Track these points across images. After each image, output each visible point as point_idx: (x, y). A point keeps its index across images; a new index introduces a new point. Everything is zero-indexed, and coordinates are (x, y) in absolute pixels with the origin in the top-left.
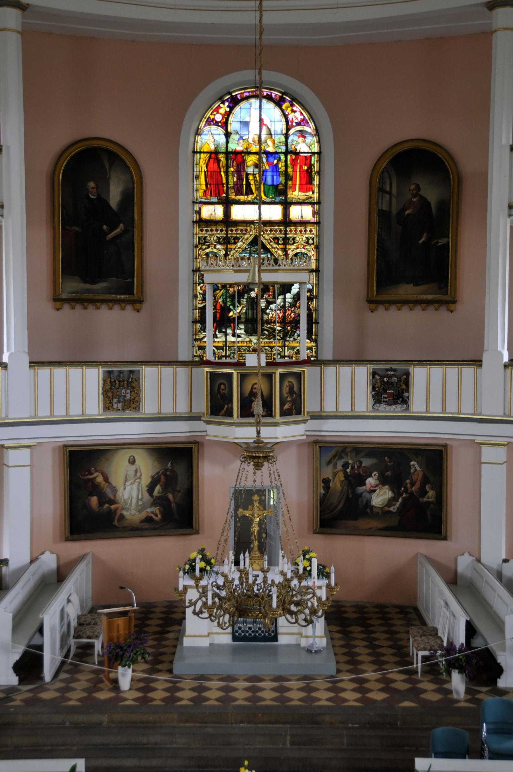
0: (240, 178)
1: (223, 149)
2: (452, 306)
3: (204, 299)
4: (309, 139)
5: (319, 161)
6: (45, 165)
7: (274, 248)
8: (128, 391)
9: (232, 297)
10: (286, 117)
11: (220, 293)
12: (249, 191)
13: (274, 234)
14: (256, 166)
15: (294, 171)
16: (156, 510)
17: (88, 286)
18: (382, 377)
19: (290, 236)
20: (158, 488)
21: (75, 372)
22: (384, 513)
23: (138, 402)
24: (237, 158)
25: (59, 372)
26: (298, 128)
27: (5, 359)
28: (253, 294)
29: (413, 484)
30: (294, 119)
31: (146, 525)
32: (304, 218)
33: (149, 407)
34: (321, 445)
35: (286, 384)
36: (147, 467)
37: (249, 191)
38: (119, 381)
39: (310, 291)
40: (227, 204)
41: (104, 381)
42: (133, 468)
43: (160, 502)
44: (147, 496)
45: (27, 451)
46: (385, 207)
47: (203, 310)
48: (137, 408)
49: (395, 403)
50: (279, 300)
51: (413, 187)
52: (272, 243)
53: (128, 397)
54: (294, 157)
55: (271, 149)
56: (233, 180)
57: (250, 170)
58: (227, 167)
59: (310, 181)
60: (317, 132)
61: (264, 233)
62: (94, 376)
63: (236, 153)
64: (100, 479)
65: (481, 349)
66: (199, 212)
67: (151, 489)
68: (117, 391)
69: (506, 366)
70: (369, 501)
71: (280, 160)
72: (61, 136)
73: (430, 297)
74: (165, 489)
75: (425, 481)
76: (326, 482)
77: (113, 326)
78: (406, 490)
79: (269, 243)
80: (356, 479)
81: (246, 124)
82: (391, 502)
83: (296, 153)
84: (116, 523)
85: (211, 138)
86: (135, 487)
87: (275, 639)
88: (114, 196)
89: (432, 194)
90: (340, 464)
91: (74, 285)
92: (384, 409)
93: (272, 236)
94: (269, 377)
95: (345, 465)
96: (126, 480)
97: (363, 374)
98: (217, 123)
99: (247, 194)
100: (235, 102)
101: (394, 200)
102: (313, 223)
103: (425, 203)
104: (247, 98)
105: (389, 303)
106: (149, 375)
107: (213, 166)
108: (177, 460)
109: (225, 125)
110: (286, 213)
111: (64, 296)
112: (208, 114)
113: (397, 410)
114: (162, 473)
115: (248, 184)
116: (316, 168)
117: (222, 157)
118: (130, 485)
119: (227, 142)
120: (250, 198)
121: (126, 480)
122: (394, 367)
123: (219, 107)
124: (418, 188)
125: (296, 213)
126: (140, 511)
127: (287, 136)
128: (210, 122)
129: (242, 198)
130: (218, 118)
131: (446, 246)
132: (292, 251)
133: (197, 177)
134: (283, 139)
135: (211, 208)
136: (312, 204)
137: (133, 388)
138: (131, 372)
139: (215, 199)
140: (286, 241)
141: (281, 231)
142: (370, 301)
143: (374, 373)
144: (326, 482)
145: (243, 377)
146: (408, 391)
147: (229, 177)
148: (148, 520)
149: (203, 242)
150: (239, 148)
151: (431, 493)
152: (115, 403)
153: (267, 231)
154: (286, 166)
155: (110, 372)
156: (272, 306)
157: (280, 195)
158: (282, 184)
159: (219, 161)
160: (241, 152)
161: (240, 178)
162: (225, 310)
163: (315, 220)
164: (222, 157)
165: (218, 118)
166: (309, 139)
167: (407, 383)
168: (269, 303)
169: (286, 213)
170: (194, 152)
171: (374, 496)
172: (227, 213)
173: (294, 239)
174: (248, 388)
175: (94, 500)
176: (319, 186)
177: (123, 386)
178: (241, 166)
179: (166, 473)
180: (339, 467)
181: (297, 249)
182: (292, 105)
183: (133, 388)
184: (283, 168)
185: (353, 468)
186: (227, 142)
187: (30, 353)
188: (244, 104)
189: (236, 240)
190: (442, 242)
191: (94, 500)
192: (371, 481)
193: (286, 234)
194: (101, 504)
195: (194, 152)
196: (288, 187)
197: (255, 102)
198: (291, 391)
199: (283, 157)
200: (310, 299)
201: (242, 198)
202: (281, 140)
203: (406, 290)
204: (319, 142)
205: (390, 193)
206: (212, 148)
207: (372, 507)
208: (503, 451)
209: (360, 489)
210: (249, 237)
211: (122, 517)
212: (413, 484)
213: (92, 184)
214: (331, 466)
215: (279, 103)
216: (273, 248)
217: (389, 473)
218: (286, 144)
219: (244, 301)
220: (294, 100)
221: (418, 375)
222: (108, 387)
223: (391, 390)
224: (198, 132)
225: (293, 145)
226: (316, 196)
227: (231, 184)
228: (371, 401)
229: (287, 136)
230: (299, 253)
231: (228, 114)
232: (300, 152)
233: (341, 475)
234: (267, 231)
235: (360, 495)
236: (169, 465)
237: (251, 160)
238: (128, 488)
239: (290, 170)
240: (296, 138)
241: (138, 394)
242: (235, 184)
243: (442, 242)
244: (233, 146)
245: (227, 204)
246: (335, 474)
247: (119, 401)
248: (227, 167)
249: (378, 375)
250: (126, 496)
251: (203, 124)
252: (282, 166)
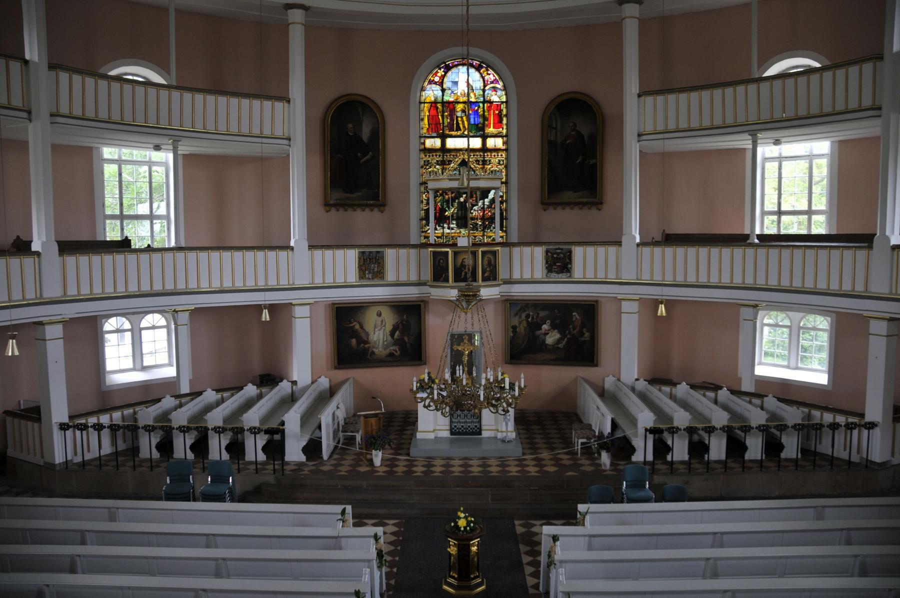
0: (452, 120)
1: (440, 100)
2: (600, 206)
3: (428, 204)
4: (499, 93)
5: (507, 107)
6: (318, 113)
9: (447, 202)
10: (483, 78)
11: (439, 199)
12: (458, 129)
14: (463, 111)
15: (490, 114)
16: (396, 348)
17: (348, 195)
18: (553, 254)
20: (397, 333)
21: (340, 253)
22: (554, 348)
23: (383, 273)
24: (450, 106)
25: (329, 253)
26: (492, 85)
27: (292, 244)
28: (462, 200)
29: (574, 328)
31: (389, 359)
33: (390, 276)
35: (486, 258)
36: (389, 319)
37: (458, 129)
39: (502, 197)
40: (443, 137)
41: (359, 258)
42: (380, 319)
43: (399, 342)
44: (389, 338)
45: (308, 307)
46: (553, 138)
47: (427, 211)
48: (382, 278)
49: (562, 272)
50: (480, 203)
51: (571, 124)
53: (376, 269)
55: (473, 100)
56: (447, 121)
57: (459, 114)
58: (443, 112)
59: (501, 121)
60: (505, 88)
62: (352, 255)
63: (449, 102)
64: (357, 327)
65: (621, 234)
66: (424, 144)
67: (392, 333)
69: (638, 245)
70: (544, 341)
72: (330, 93)
73: (585, 200)
74: (402, 333)
75: (583, 326)
76: (514, 328)
77: (365, 221)
78: (570, 333)
80: (535, 326)
81: (456, 83)
82: (559, 341)
83: (491, 102)
84: (369, 357)
85: (432, 93)
86: (381, 332)
87: (480, 434)
88: (366, 133)
89: (585, 129)
90: (524, 316)
91: (338, 195)
92: (554, 276)
94: (474, 254)
95: (528, 316)
96: (375, 327)
97: (539, 252)
98: (435, 83)
99: (457, 130)
100: (448, 69)
101: (559, 134)
102: (503, 150)
103: (580, 136)
104: (456, 66)
105: (556, 205)
106: (390, 254)
107: (433, 112)
108: (410, 314)
109: (441, 84)
110: (484, 143)
111: (331, 202)
112: (430, 77)
113: (563, 277)
115: (458, 124)
116: (504, 112)
117: (439, 106)
118: (378, 331)
119: (443, 95)
120: (459, 133)
121: (375, 327)
122: (561, 247)
123: (437, 72)
124: (575, 125)
125: (491, 143)
126: (385, 349)
127: (484, 91)
128: (431, 82)
129: (453, 133)
130: (437, 79)
131: (595, 165)
133: (423, 120)
134: (481, 93)
135: (433, 140)
136: (502, 137)
138: (378, 252)
139: (434, 135)
140: (484, 162)
142: (543, 203)
143: (547, 252)
144: (514, 328)
145: (456, 254)
146: (571, 263)
147: (445, 118)
148: (391, 355)
149: (427, 163)
150: (451, 99)
151: (587, 334)
154: (484, 111)
155: (363, 253)
156: (476, 208)
157: (480, 130)
159: (437, 108)
160: (452, 102)
161: (452, 120)
162: (443, 210)
163: (504, 147)
164: (439, 106)
165: (437, 79)
166: (499, 93)
167: (570, 258)
168: (473, 206)
169: (484, 143)
170: (420, 103)
171: (547, 337)
172: (443, 143)
174: (459, 261)
175: (354, 341)
176: (507, 124)
178: (453, 111)
180: (523, 317)
182: (487, 70)
185: (533, 318)
186: (443, 95)
187: (308, 239)
188: (454, 70)
189: (450, 162)
190: (592, 162)
191: (354, 341)
192: (545, 327)
194: (358, 343)
195: (420, 103)
197: (463, 69)
198: (490, 264)
199: (481, 105)
200: (502, 202)
201: (453, 133)
203: (569, 196)
204: (506, 94)
205: (556, 128)
206: (433, 99)
207: (547, 345)
208: (636, 304)
209: (539, 332)
210: (458, 160)
211: (373, 353)
212: (574, 328)
213: (350, 125)
214: (517, 317)
215: (478, 69)
217: (558, 321)
219: (456, 205)
220: (489, 67)
221: (578, 252)
223: (559, 263)
224: (423, 89)
226: (505, 131)
227: (446, 124)
228: (545, 271)
231: (443, 77)
233: (525, 322)
235: (538, 337)
237: (459, 107)
238: (377, 333)
239: (486, 113)
240: (490, 92)
241: (383, 268)
242: (449, 123)
243: (592, 162)
244: (446, 98)
245: (443, 137)
246: (520, 323)
247: (370, 273)
248: (443, 112)
250: (375, 339)
251: (426, 83)
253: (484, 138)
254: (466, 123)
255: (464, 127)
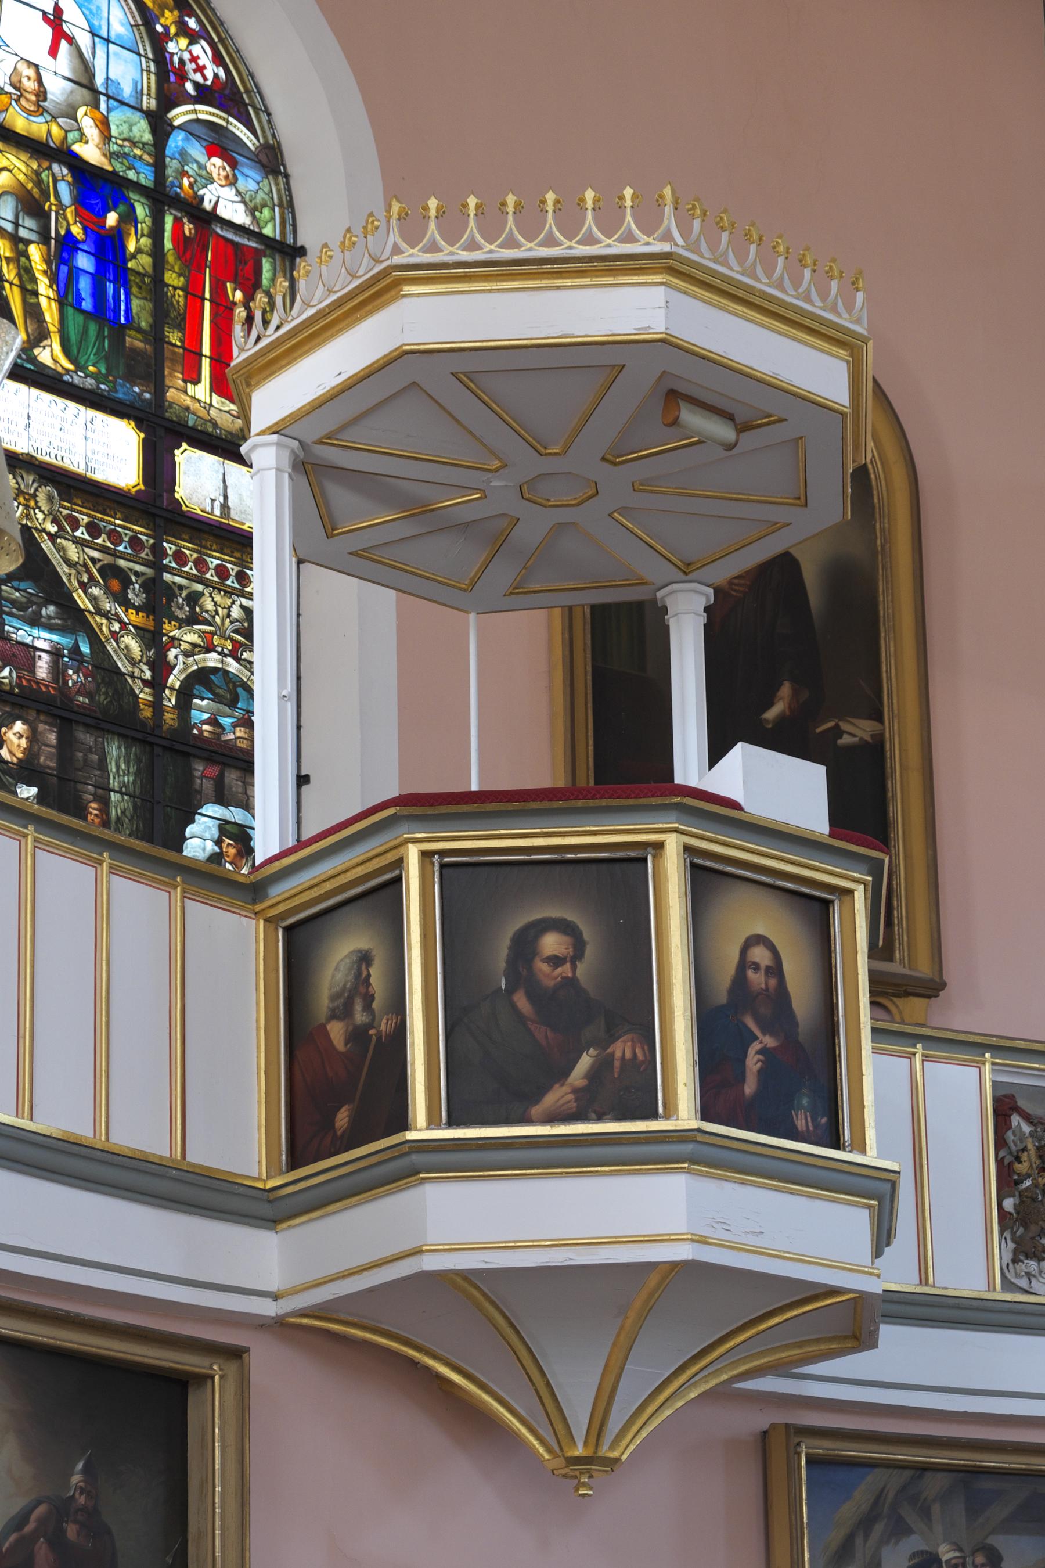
7: (105, 615)
13: (103, 549)
15: (194, 292)
19: (178, 580)
26: (205, 112)
30: (190, 67)
32: (233, 515)
34: (821, 1447)
52: (95, 591)
54: (188, 228)
61: (61, 528)
71: (129, 217)
79: (83, 586)
93: (96, 554)
114: (42, 1521)
127: (159, 124)
132: (187, 654)
134: (142, 130)
140: (158, 601)
141: (135, 542)
143: (1005, 1107)
153: (75, 524)
158: (139, 330)
173: (194, 599)
179: (61, 1532)
181: (209, 649)
184: (145, 261)
193: (160, 569)
196: (167, 354)
202: (136, 132)
216: (99, 612)
218: (159, 166)
225: (184, 174)
228: (1001, 1253)
229: (159, 124)
230: (215, 670)
232: (212, 217)
234: (75, 524)
236: (76, 1479)
239: (172, 278)
240: (197, 151)
249: (1027, 1118)
252: (139, 251)
253: (164, 434)
254: (44, 286)
255: (33, 312)
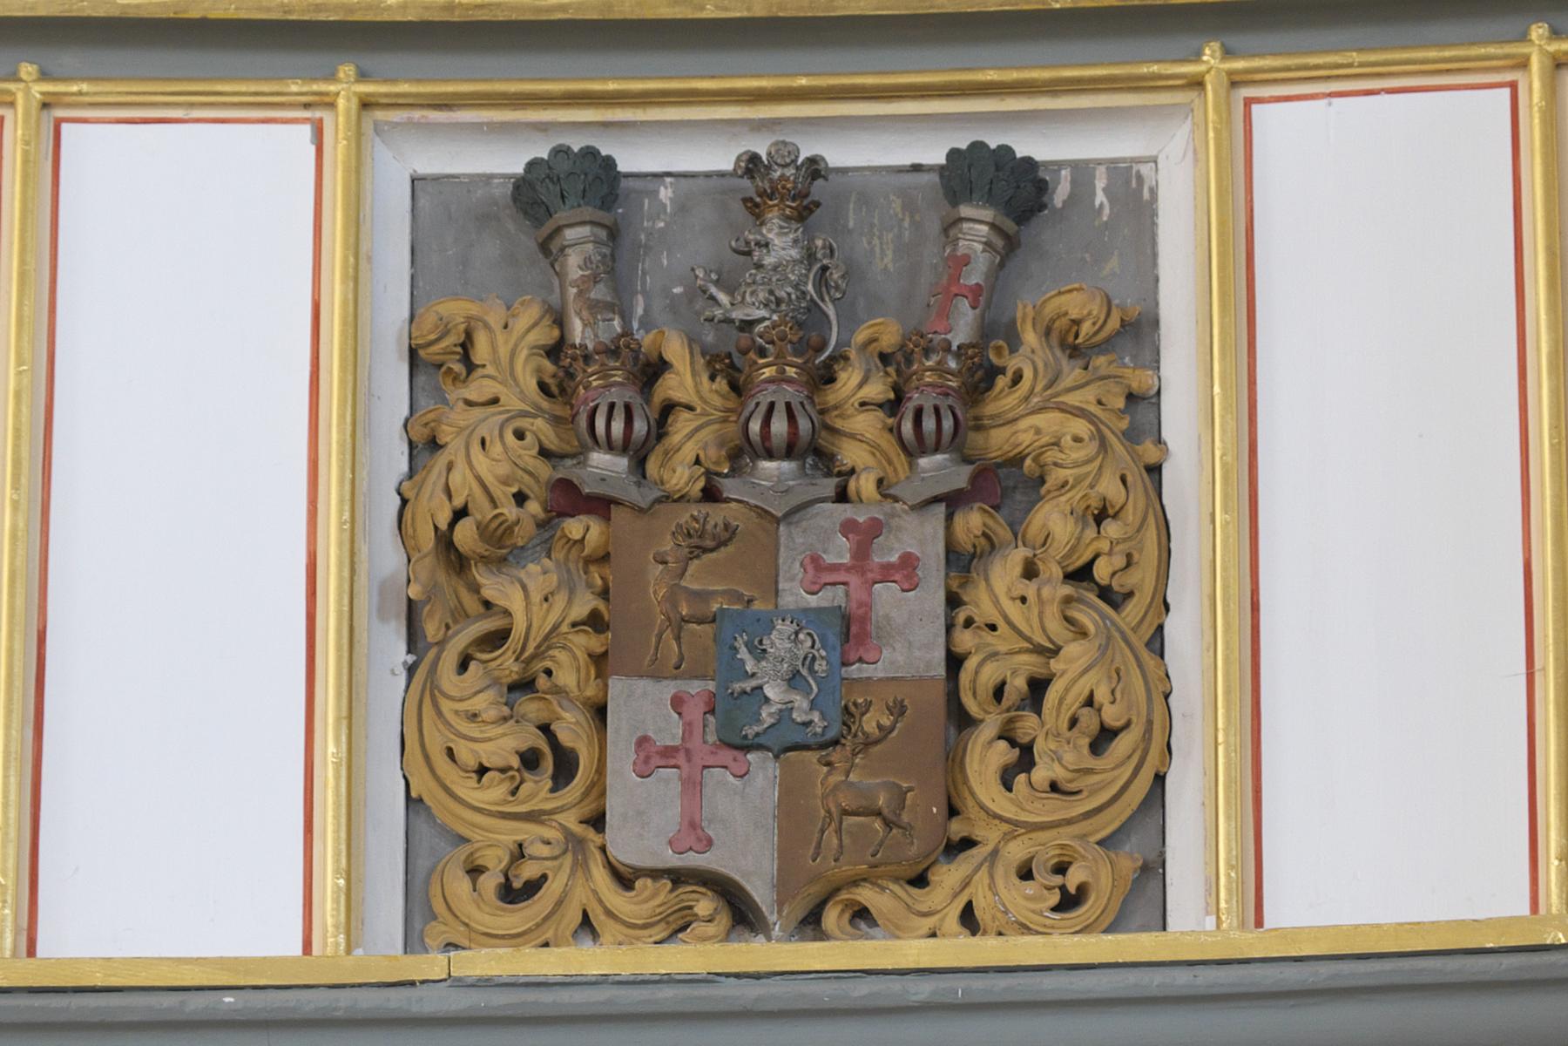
8: (921, 537)
23: (1130, 742)
38: (730, 370)
41: (438, 362)
68: (699, 544)
137: (1005, 484)
152: (651, 756)
177: (814, 452)
183: (1005, 484)
222: (490, 463)
241: (1114, 591)
